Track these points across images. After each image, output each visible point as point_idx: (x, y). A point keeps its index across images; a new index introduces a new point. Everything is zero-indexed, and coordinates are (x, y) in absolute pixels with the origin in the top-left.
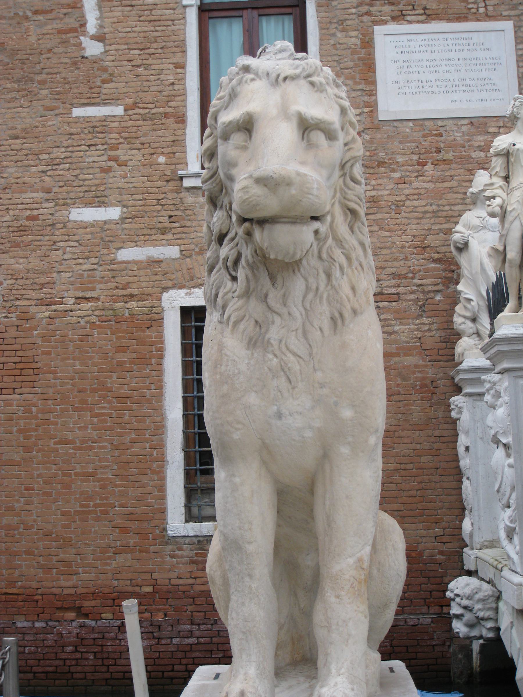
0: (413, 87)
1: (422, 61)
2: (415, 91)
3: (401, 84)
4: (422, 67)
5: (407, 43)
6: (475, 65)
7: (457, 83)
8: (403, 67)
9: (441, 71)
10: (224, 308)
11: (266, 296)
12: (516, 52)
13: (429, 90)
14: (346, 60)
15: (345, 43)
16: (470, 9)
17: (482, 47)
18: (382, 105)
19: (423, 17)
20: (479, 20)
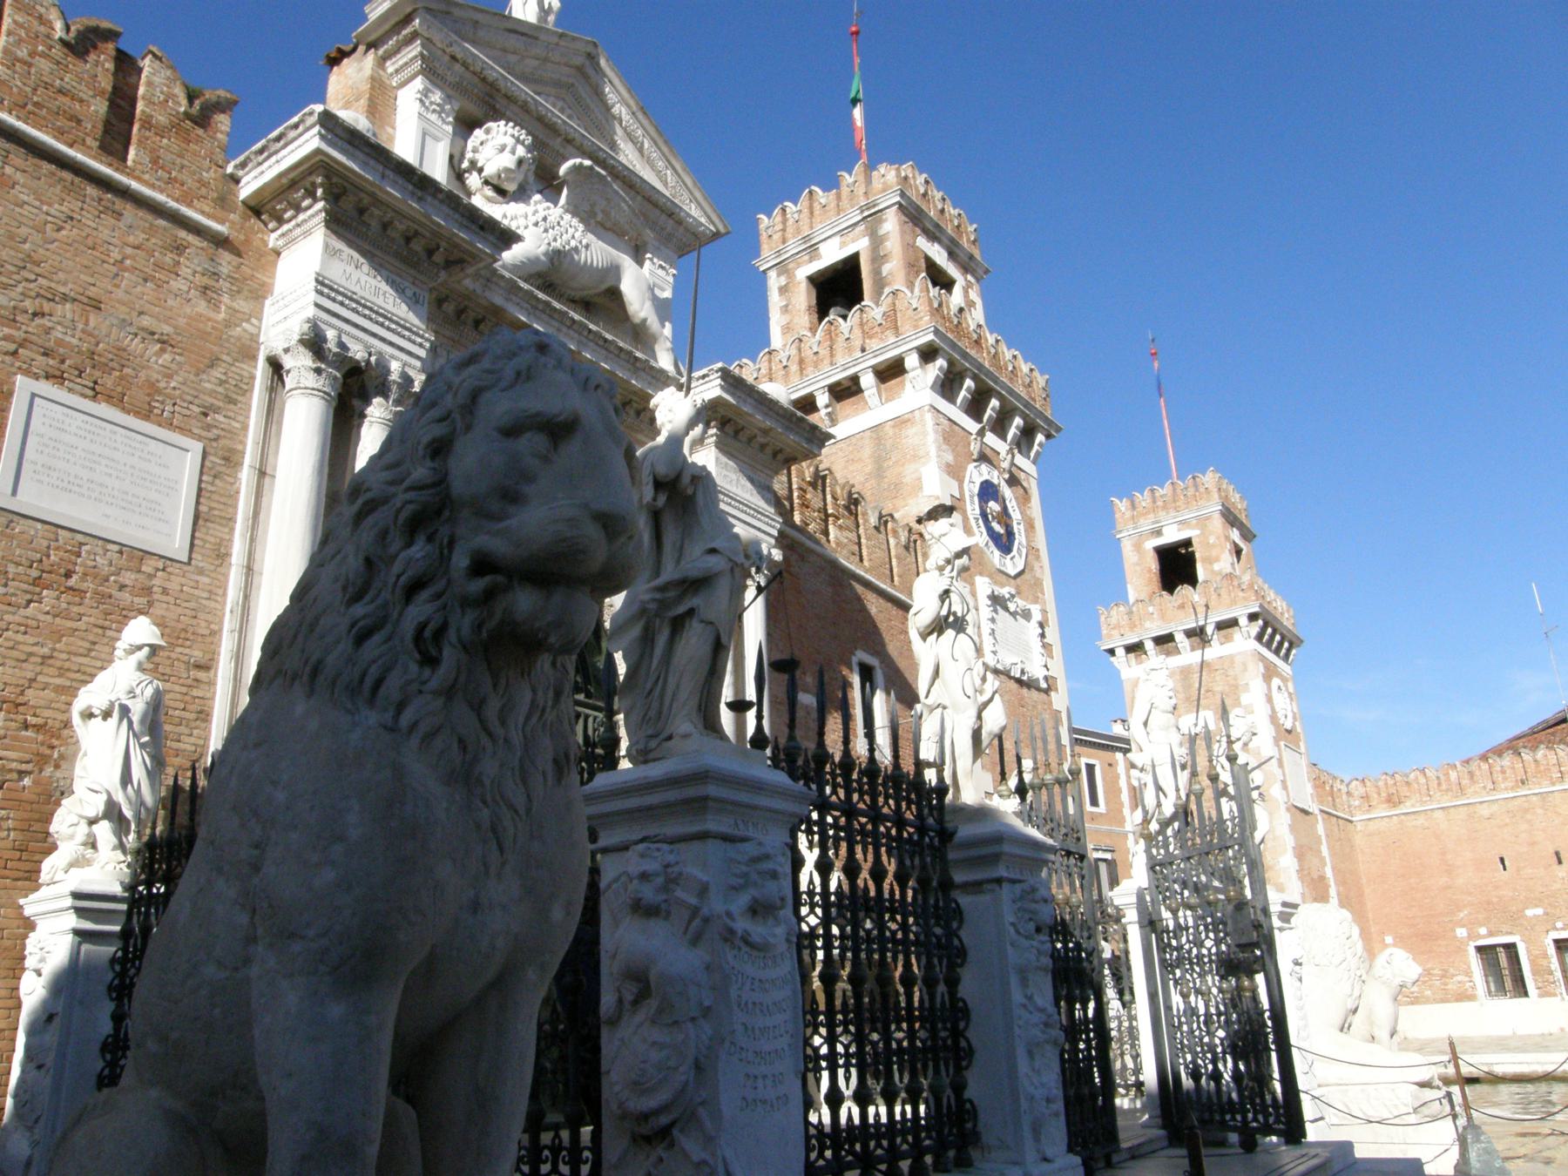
3: (39, 467)
10: (400, 707)
11: (483, 701)
13: (76, 488)
19: (91, 393)
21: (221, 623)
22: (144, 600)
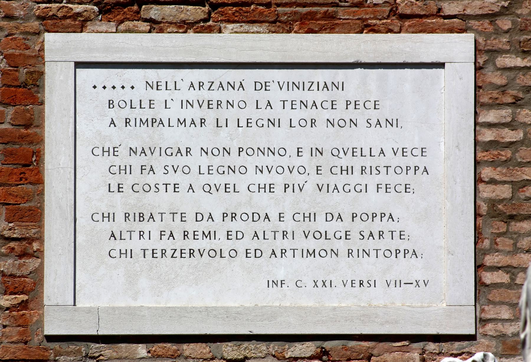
0: (155, 235)
1: (188, 151)
2: (159, 246)
4: (186, 170)
5: (142, 93)
6: (348, 170)
7: (288, 225)
8: (127, 170)
9: (242, 187)
17: (374, 115)
18: (55, 287)
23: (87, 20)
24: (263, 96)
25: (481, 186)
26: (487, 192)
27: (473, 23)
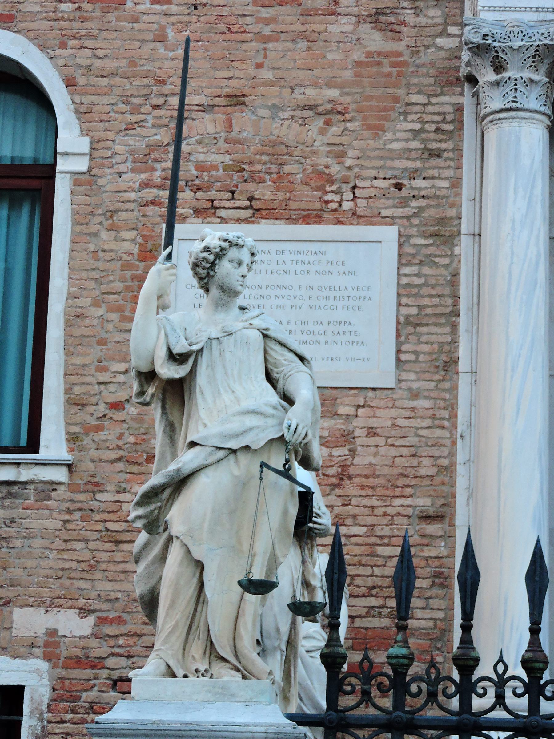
6: (327, 298)
12: (399, 279)
14: (111, 278)
15: (112, 251)
16: (327, 202)
17: (342, 269)
19: (247, 213)
20: (339, 222)
21: (452, 454)
22: (345, 451)
23: (186, 217)
24: (281, 258)
25: (401, 308)
26: (404, 311)
27: (397, 221)
